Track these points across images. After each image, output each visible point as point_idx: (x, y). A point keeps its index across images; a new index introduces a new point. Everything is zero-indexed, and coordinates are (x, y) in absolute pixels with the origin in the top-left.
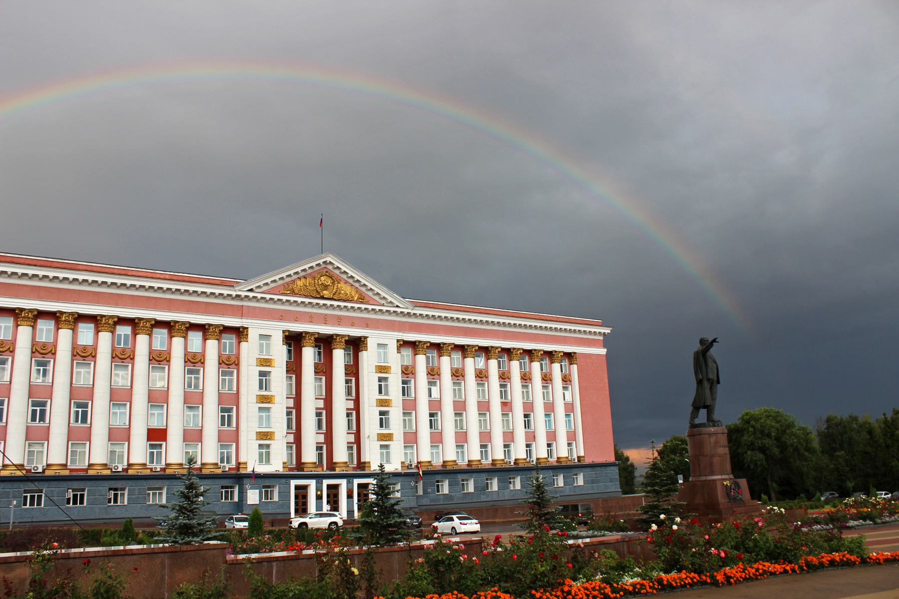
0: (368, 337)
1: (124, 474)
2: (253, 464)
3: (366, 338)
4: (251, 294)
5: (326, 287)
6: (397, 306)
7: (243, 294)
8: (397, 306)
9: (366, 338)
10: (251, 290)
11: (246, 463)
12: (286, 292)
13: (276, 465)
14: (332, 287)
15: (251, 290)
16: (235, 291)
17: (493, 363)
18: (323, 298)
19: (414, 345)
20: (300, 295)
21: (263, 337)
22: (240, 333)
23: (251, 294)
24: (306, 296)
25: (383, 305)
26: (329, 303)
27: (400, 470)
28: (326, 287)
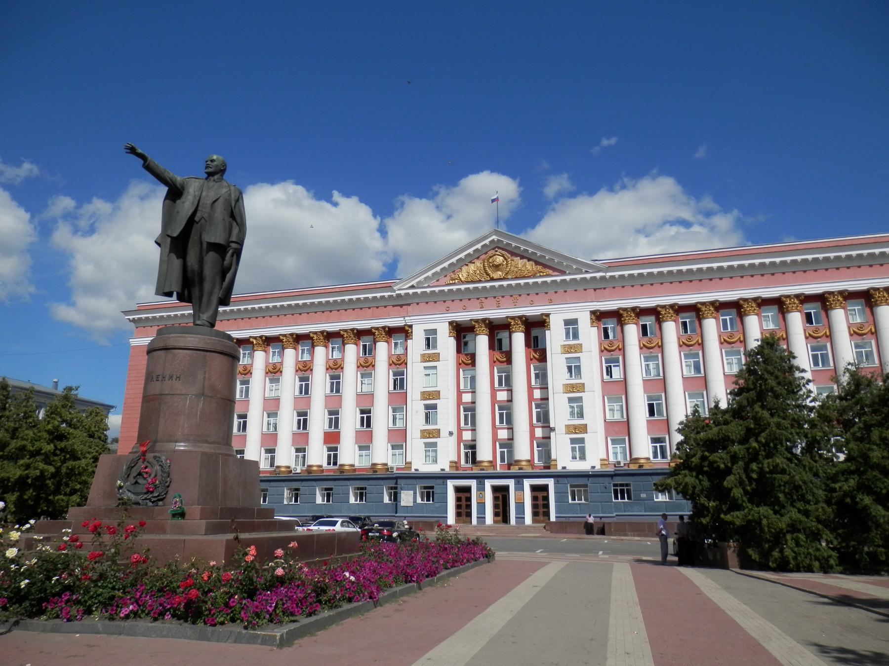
0: (550, 314)
1: (626, 468)
2: (421, 465)
3: (548, 315)
4: (411, 291)
5: (497, 267)
6: (586, 271)
7: (402, 292)
8: (586, 271)
9: (548, 315)
10: (413, 287)
11: (410, 463)
12: (451, 282)
13: (443, 465)
14: (505, 266)
15: (413, 287)
16: (394, 291)
17: (796, 320)
18: (492, 279)
19: (618, 316)
20: (468, 282)
21: (568, 322)
22: (405, 332)
23: (411, 291)
24: (472, 282)
25: (563, 273)
26: (497, 284)
27: (598, 468)
28: (497, 267)
